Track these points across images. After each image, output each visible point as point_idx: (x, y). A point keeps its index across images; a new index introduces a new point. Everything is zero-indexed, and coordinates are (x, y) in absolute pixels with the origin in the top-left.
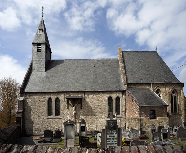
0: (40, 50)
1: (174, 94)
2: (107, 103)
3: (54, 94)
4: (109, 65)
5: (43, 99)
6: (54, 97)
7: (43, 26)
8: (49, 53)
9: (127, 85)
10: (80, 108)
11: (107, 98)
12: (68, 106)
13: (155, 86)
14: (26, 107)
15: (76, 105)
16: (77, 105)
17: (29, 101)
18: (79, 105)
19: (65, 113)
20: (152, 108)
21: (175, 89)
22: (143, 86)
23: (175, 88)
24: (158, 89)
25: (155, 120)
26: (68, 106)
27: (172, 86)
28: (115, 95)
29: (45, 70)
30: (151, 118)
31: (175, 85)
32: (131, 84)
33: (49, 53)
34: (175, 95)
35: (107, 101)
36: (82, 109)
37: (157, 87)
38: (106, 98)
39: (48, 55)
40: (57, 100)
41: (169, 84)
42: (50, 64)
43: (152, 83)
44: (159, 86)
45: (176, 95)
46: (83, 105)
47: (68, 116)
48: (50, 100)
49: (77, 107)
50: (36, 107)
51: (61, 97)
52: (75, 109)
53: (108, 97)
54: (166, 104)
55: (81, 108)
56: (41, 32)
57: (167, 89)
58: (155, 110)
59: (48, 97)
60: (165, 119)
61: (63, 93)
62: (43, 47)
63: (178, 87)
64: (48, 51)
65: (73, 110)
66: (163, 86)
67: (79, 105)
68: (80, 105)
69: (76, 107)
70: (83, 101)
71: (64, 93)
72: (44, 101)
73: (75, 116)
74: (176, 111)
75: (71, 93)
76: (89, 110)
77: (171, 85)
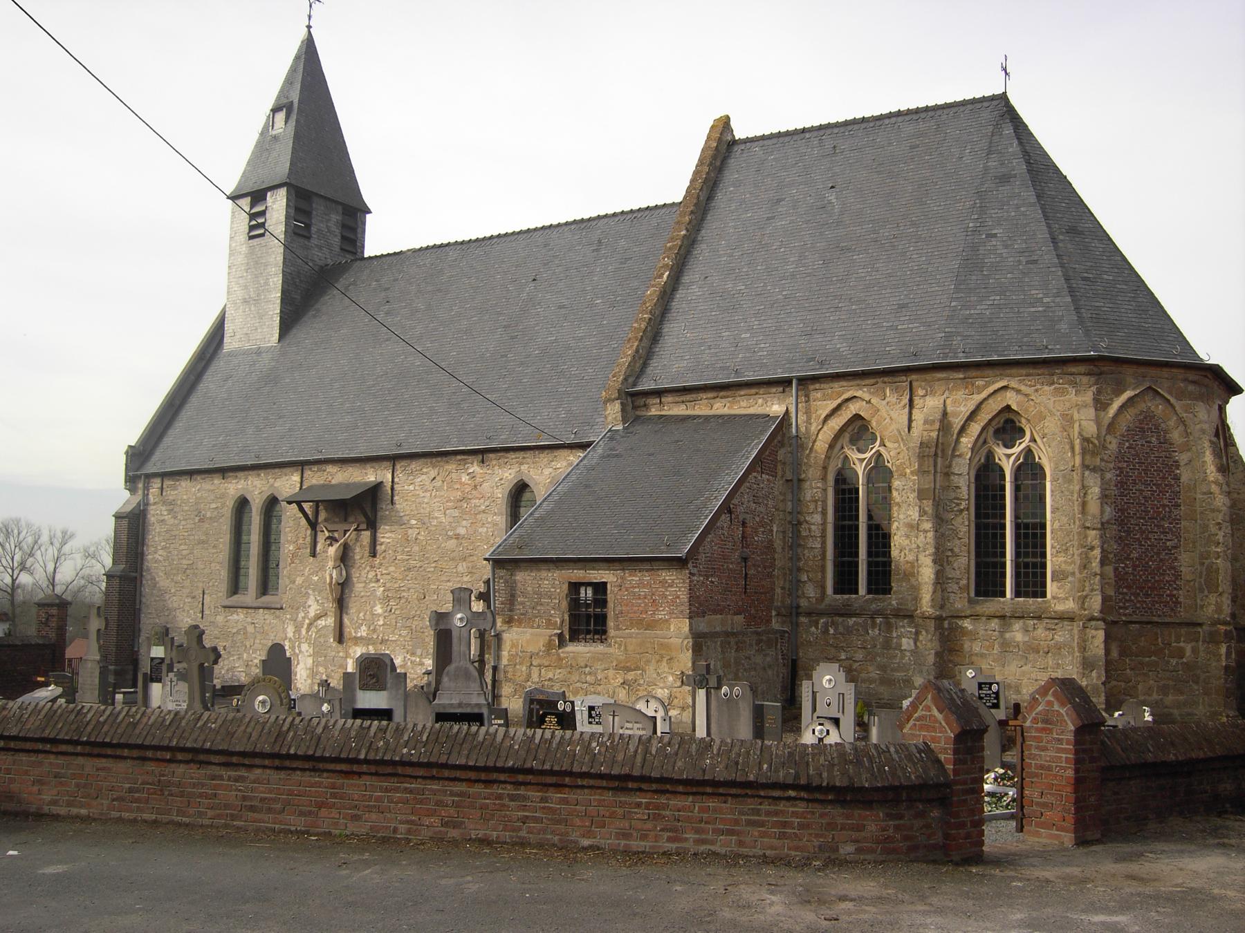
5: (214, 506)
6: (256, 488)
11: (501, 494)
17: (157, 513)
19: (299, 580)
22: (744, 404)
23: (1011, 399)
24: (857, 417)
28: (547, 471)
31: (1002, 376)
36: (377, 561)
44: (859, 394)
46: (386, 536)
47: (311, 601)
48: (242, 504)
51: (288, 484)
52: (345, 558)
53: (508, 486)
55: (374, 554)
57: (929, 404)
59: (234, 487)
71: (301, 465)
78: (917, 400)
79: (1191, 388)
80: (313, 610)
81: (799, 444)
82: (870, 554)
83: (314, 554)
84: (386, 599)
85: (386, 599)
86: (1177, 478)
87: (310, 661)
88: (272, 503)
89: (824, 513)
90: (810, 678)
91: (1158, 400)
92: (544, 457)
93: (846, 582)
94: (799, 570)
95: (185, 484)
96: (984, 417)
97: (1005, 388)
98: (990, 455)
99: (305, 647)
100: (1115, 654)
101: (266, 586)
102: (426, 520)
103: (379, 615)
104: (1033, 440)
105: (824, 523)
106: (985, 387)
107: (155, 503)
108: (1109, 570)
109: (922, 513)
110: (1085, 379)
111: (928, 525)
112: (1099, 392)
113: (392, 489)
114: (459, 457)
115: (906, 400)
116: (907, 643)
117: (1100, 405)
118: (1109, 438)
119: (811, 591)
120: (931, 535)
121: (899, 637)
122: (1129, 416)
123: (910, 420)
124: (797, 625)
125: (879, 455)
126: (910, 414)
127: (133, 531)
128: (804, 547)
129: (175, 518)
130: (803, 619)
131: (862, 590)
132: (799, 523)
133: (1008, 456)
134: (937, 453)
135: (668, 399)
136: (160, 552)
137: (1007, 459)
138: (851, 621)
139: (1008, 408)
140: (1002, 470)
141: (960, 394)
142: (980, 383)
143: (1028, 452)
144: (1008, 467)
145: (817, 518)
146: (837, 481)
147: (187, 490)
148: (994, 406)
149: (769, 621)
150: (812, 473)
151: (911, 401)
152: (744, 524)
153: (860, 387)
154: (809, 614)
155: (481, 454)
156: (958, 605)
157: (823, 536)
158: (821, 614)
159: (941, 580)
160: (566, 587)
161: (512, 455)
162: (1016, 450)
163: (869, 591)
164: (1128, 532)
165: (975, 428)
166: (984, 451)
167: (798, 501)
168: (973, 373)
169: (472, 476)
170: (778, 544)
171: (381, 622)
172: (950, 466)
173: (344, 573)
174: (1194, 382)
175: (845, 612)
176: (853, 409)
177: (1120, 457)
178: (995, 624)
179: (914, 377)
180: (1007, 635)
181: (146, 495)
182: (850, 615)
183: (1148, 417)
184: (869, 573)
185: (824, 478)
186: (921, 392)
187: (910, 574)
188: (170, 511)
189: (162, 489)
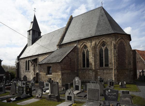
6: (27, 60)
12: (32, 65)
13: (81, 43)
23: (104, 40)
24: (85, 45)
26: (32, 65)
27: (100, 39)
31: (102, 37)
37: (83, 43)
41: (95, 38)
44: (85, 42)
48: (26, 61)
51: (30, 59)
52: (34, 66)
57: (93, 43)
59: (26, 60)
63: (109, 38)
66: (89, 41)
79: (127, 38)
80: (32, 72)
81: (78, 49)
82: (87, 62)
86: (125, 50)
88: (29, 61)
89: (81, 58)
90: (74, 79)
91: (123, 39)
93: (84, 66)
94: (78, 65)
96: (100, 43)
97: (103, 39)
98: (101, 48)
100: (118, 74)
101: (29, 70)
104: (107, 46)
105: (81, 59)
106: (101, 39)
108: (117, 62)
109: (93, 56)
110: (114, 37)
111: (93, 58)
112: (115, 38)
115: (90, 42)
116: (91, 73)
117: (116, 40)
118: (117, 44)
119: (80, 67)
120: (94, 59)
121: (90, 73)
122: (119, 41)
123: (91, 44)
124: (78, 71)
125: (88, 49)
126: (91, 44)
127: (18, 64)
128: (79, 62)
130: (79, 71)
131: (86, 67)
132: (78, 59)
133: (104, 48)
134: (95, 48)
135: (64, 45)
137: (104, 48)
138: (84, 71)
139: (103, 41)
140: (103, 50)
142: (100, 38)
143: (106, 47)
144: (104, 49)
145: (80, 58)
146: (83, 54)
147: (22, 60)
148: (102, 41)
149: (74, 71)
150: (80, 52)
151: (91, 42)
152: (70, 58)
153: (85, 41)
154: (79, 70)
156: (97, 68)
157: (81, 60)
158: (81, 70)
159: (95, 65)
162: (105, 47)
163: (87, 67)
164: (119, 57)
165: (99, 44)
166: (101, 47)
167: (78, 56)
168: (99, 37)
170: (76, 62)
172: (96, 50)
174: (127, 37)
175: (84, 70)
177: (118, 47)
178: (102, 70)
179: (91, 38)
180: (104, 72)
182: (85, 70)
183: (121, 42)
184: (87, 65)
185: (81, 53)
186: (92, 40)
187: (91, 64)
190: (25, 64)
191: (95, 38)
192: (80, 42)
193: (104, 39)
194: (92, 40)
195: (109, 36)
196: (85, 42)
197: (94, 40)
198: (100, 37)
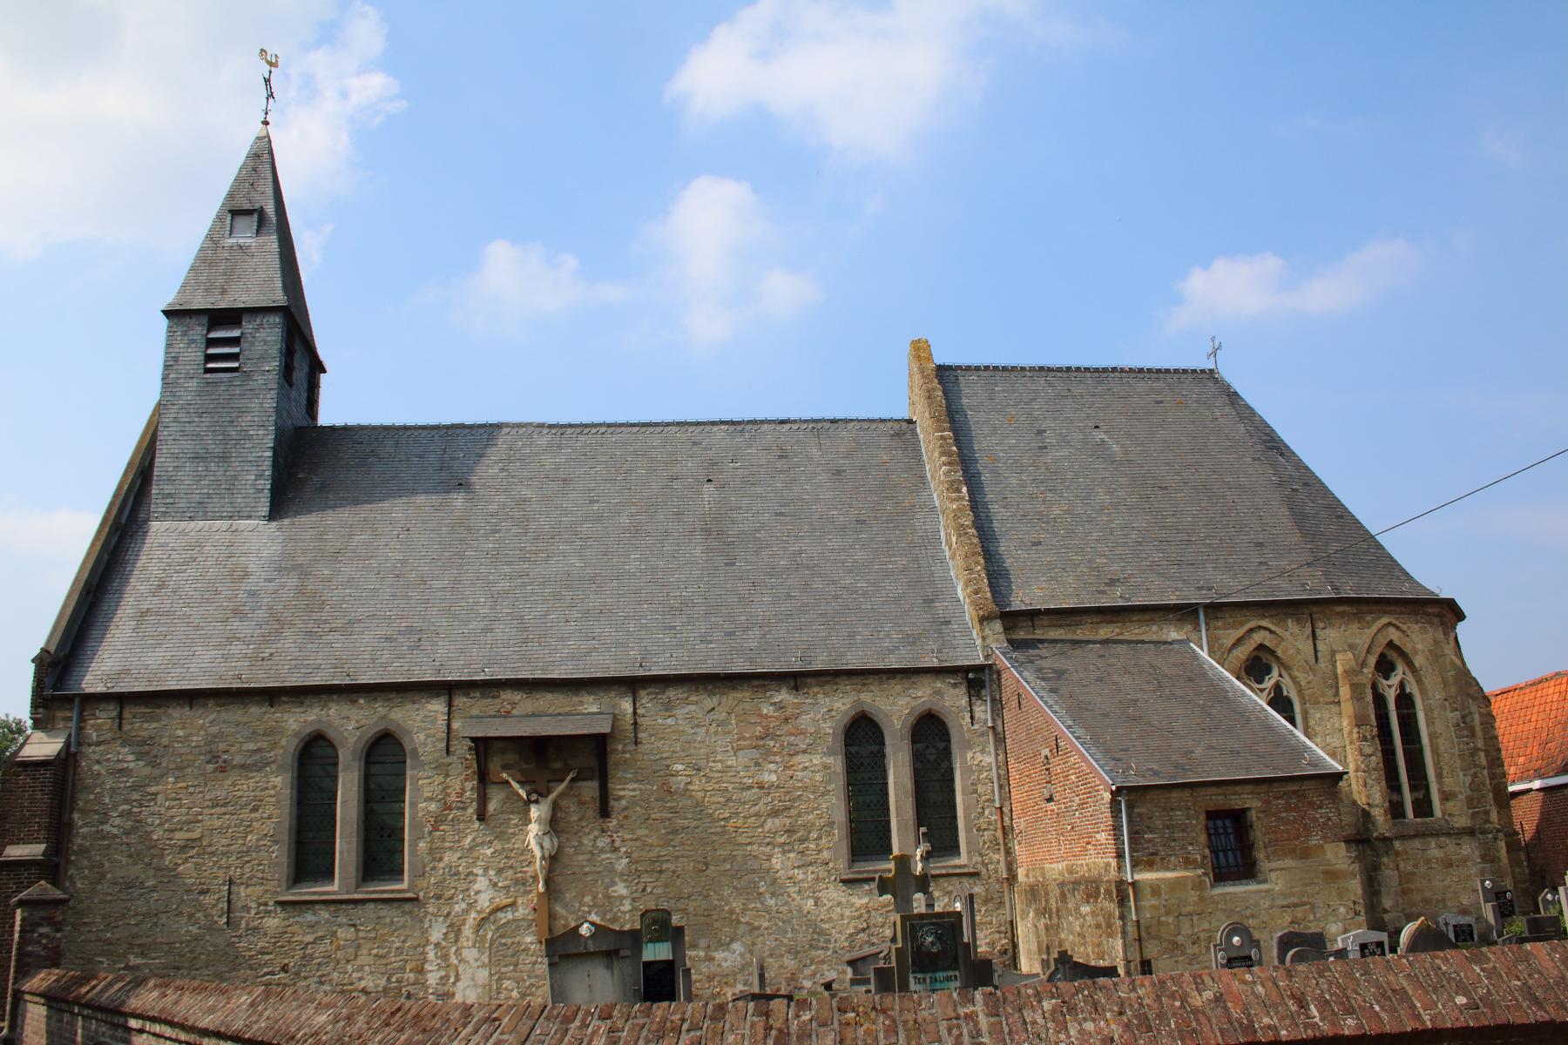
0: (234, 357)
1: (1395, 680)
2: (837, 763)
3: (354, 702)
4: (839, 472)
5: (251, 746)
7: (270, 191)
8: (300, 374)
9: (998, 626)
10: (590, 813)
12: (483, 801)
13: (1233, 627)
14: (83, 812)
15: (562, 787)
16: (570, 788)
18: (590, 789)
19: (449, 857)
20: (1217, 800)
21: (1391, 644)
23: (1394, 635)
25: (1253, 887)
26: (483, 801)
27: (1369, 625)
28: (902, 701)
29: (264, 507)
30: (1220, 876)
32: (1032, 615)
33: (300, 374)
34: (1402, 685)
35: (840, 746)
37: (1251, 630)
38: (828, 728)
39: (293, 394)
40: (385, 752)
41: (1339, 609)
42: (311, 464)
43: (1207, 607)
44: (1264, 623)
45: (1413, 688)
46: (625, 790)
47: (481, 883)
49: (569, 804)
50: (180, 814)
52: (554, 824)
54: (1332, 767)
55: (605, 812)
56: (245, 235)
57: (1332, 635)
58: (1245, 811)
59: (296, 721)
60: (1332, 876)
61: (438, 695)
62: (265, 339)
63: (1416, 627)
64: (301, 361)
65: (534, 829)
66: (1298, 621)
67: (590, 789)
68: (595, 784)
69: (555, 806)
70: (619, 748)
71: (447, 689)
72: (256, 757)
73: (547, 882)
74: (1423, 807)
75: (508, 695)
76: (681, 822)
77: (1358, 617)
78: (1318, 631)
83: (482, 817)
84: (631, 875)
85: (631, 875)
87: (483, 975)
92: (896, 686)
95: (177, 713)
97: (1390, 624)
99: (470, 954)
102: (702, 763)
103: (622, 898)
106: (1374, 620)
107: (99, 744)
110: (1436, 620)
113: (635, 724)
114: (756, 683)
115: (1308, 631)
129: (154, 764)
136: (118, 821)
141: (1354, 627)
142: (1369, 618)
151: (1313, 633)
153: (1263, 617)
155: (796, 680)
160: (1202, 817)
161: (843, 681)
168: (1365, 608)
169: (780, 707)
171: (627, 907)
173: (556, 841)
176: (1258, 638)
179: (1315, 609)
181: (80, 729)
186: (1321, 625)
188: (140, 756)
189: (120, 717)
190: (279, 784)
191: (1342, 614)
192: (1220, 624)
193: (1391, 630)
194: (1321, 625)
195: (1417, 613)
196: (1264, 623)
197: (1332, 625)
198: (1370, 612)
